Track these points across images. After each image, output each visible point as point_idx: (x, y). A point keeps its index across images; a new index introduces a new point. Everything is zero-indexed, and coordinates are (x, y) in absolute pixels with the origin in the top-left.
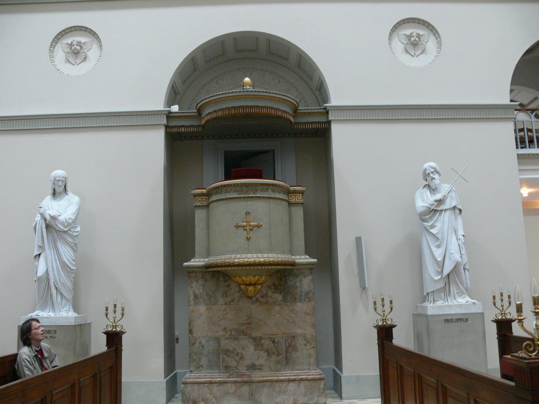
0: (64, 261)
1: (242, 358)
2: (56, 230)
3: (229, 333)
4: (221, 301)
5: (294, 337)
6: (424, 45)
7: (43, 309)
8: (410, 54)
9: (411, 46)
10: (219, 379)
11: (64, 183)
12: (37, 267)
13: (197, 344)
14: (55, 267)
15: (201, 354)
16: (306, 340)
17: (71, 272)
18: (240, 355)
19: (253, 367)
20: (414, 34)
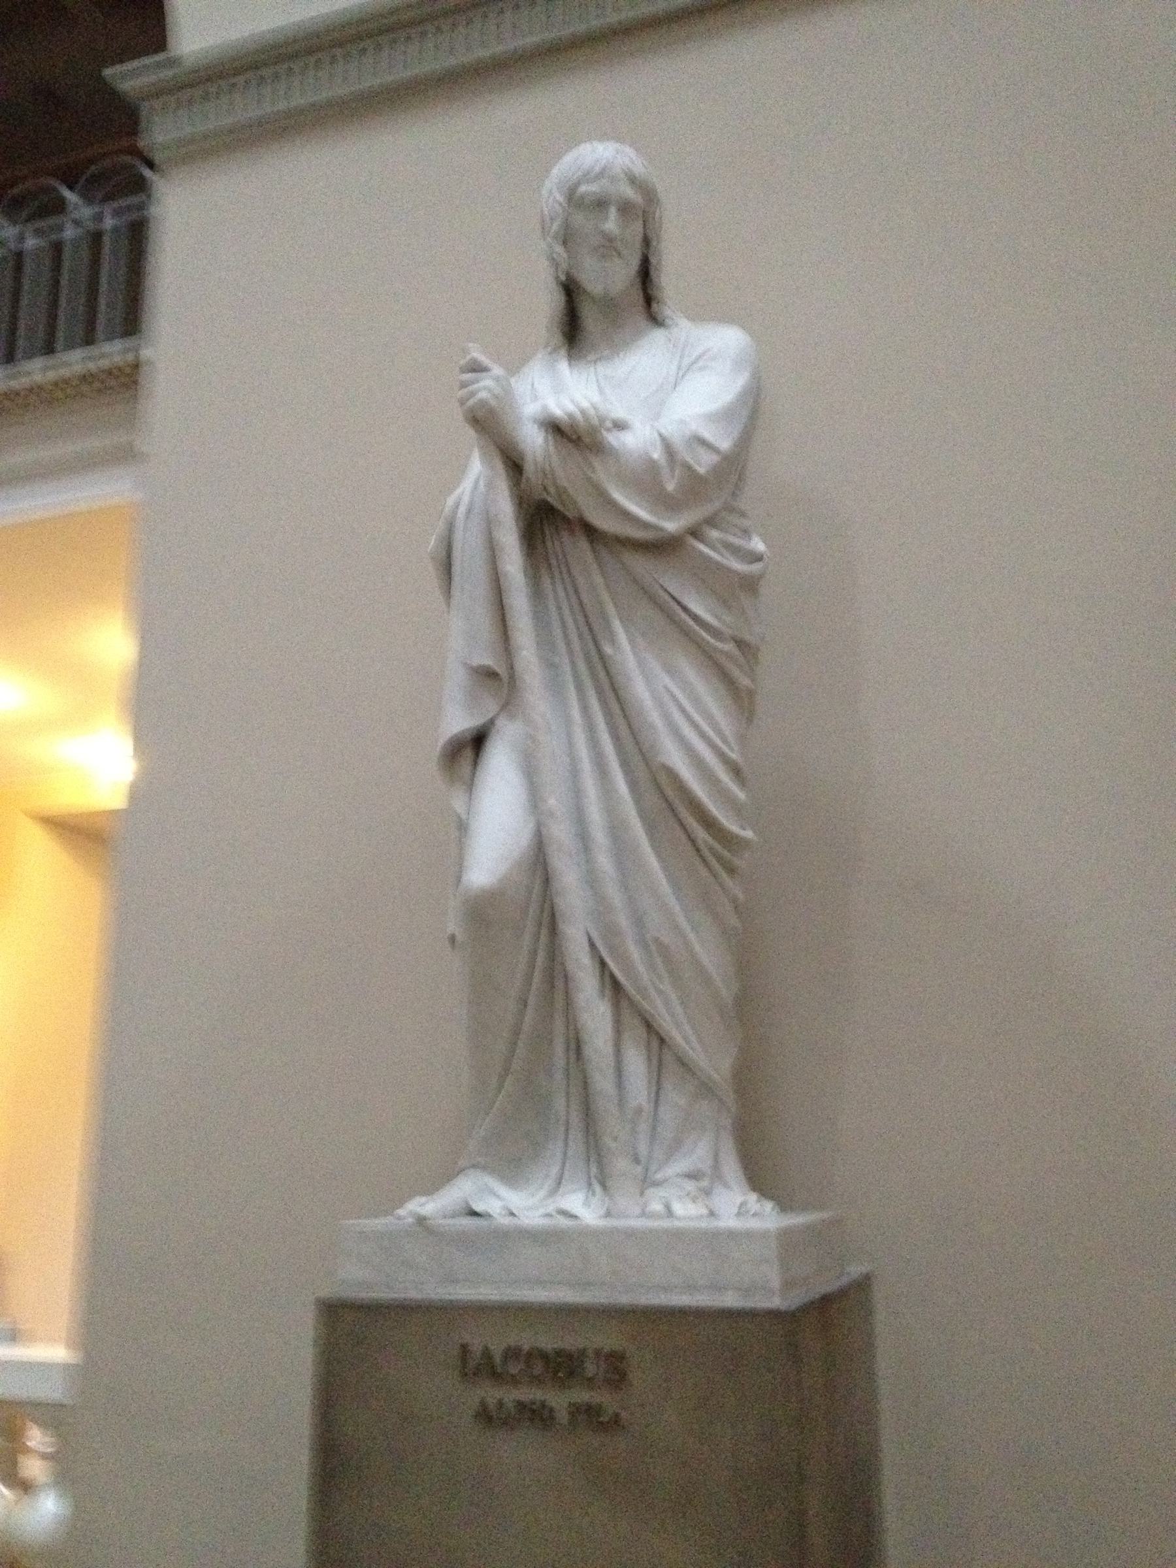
12: (463, 827)
17: (719, 858)
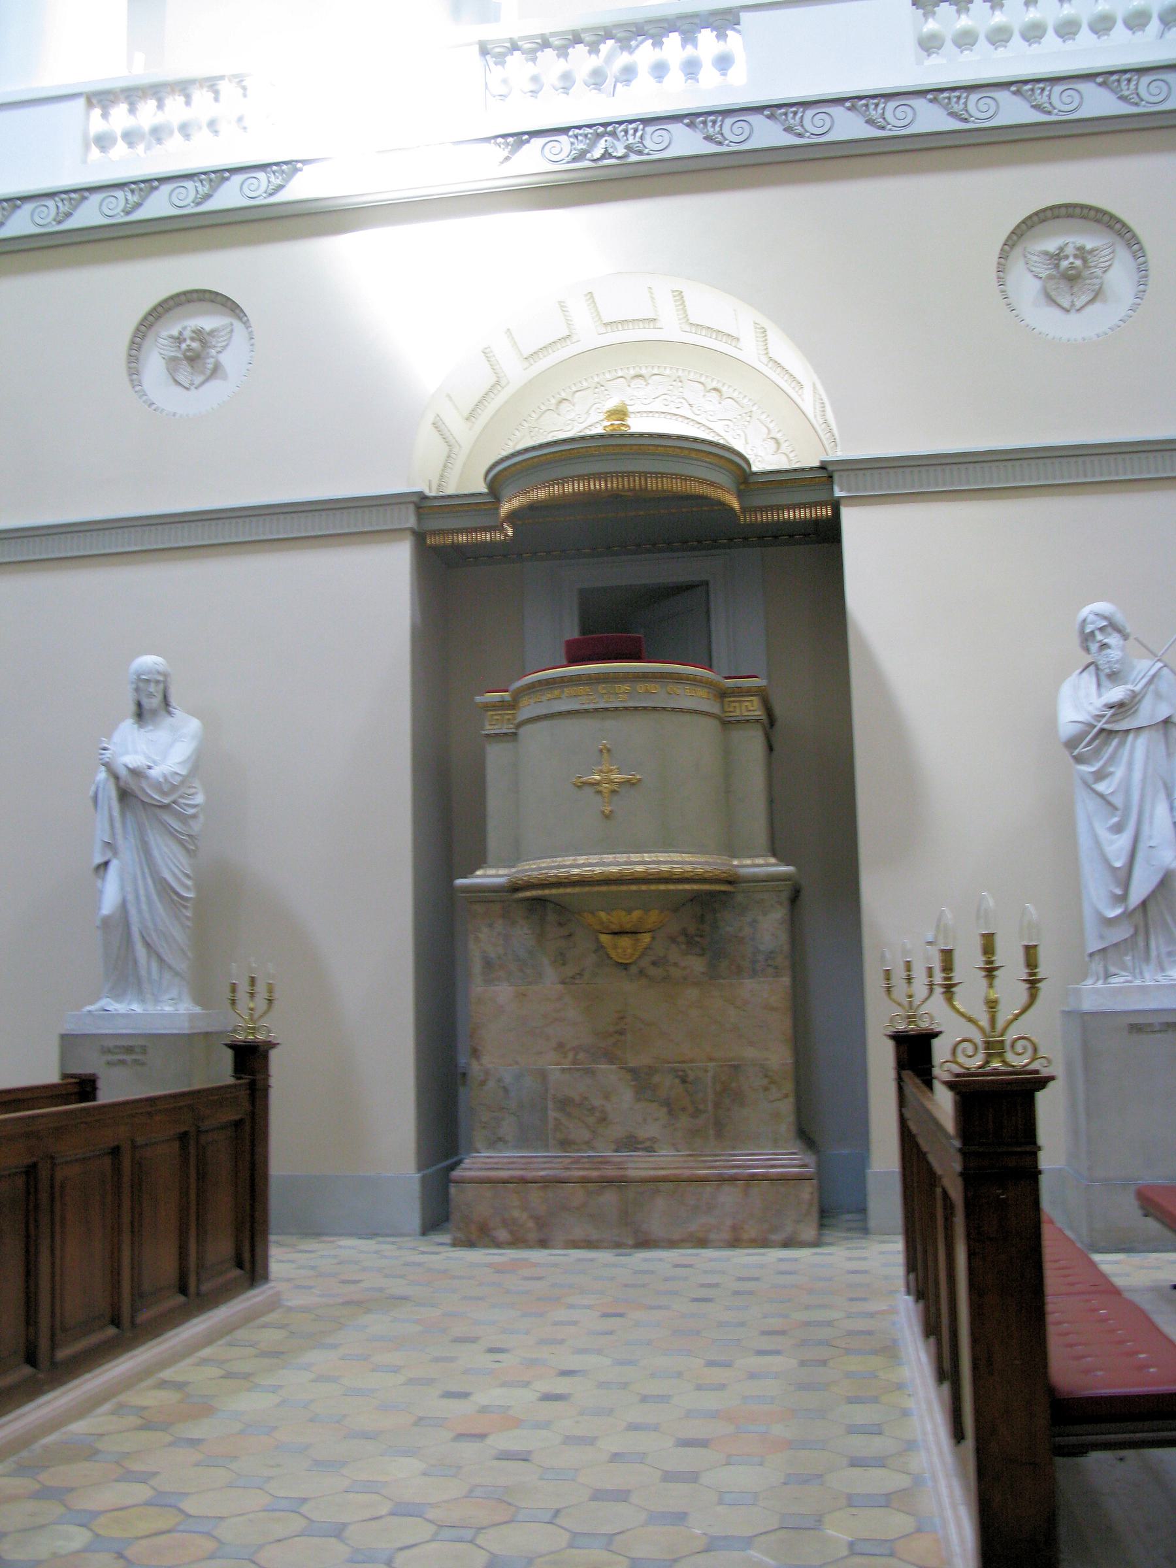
0: (165, 879)
1: (603, 1120)
2: (142, 801)
3: (570, 1055)
4: (551, 975)
5: (736, 1068)
6: (1097, 277)
7: (118, 996)
8: (1059, 305)
9: (1064, 285)
10: (542, 1173)
11: (161, 686)
12: (101, 892)
13: (491, 1084)
14: (142, 892)
15: (502, 1109)
16: (766, 1076)
18: (597, 1114)
19: (630, 1143)
20: (1070, 250)
